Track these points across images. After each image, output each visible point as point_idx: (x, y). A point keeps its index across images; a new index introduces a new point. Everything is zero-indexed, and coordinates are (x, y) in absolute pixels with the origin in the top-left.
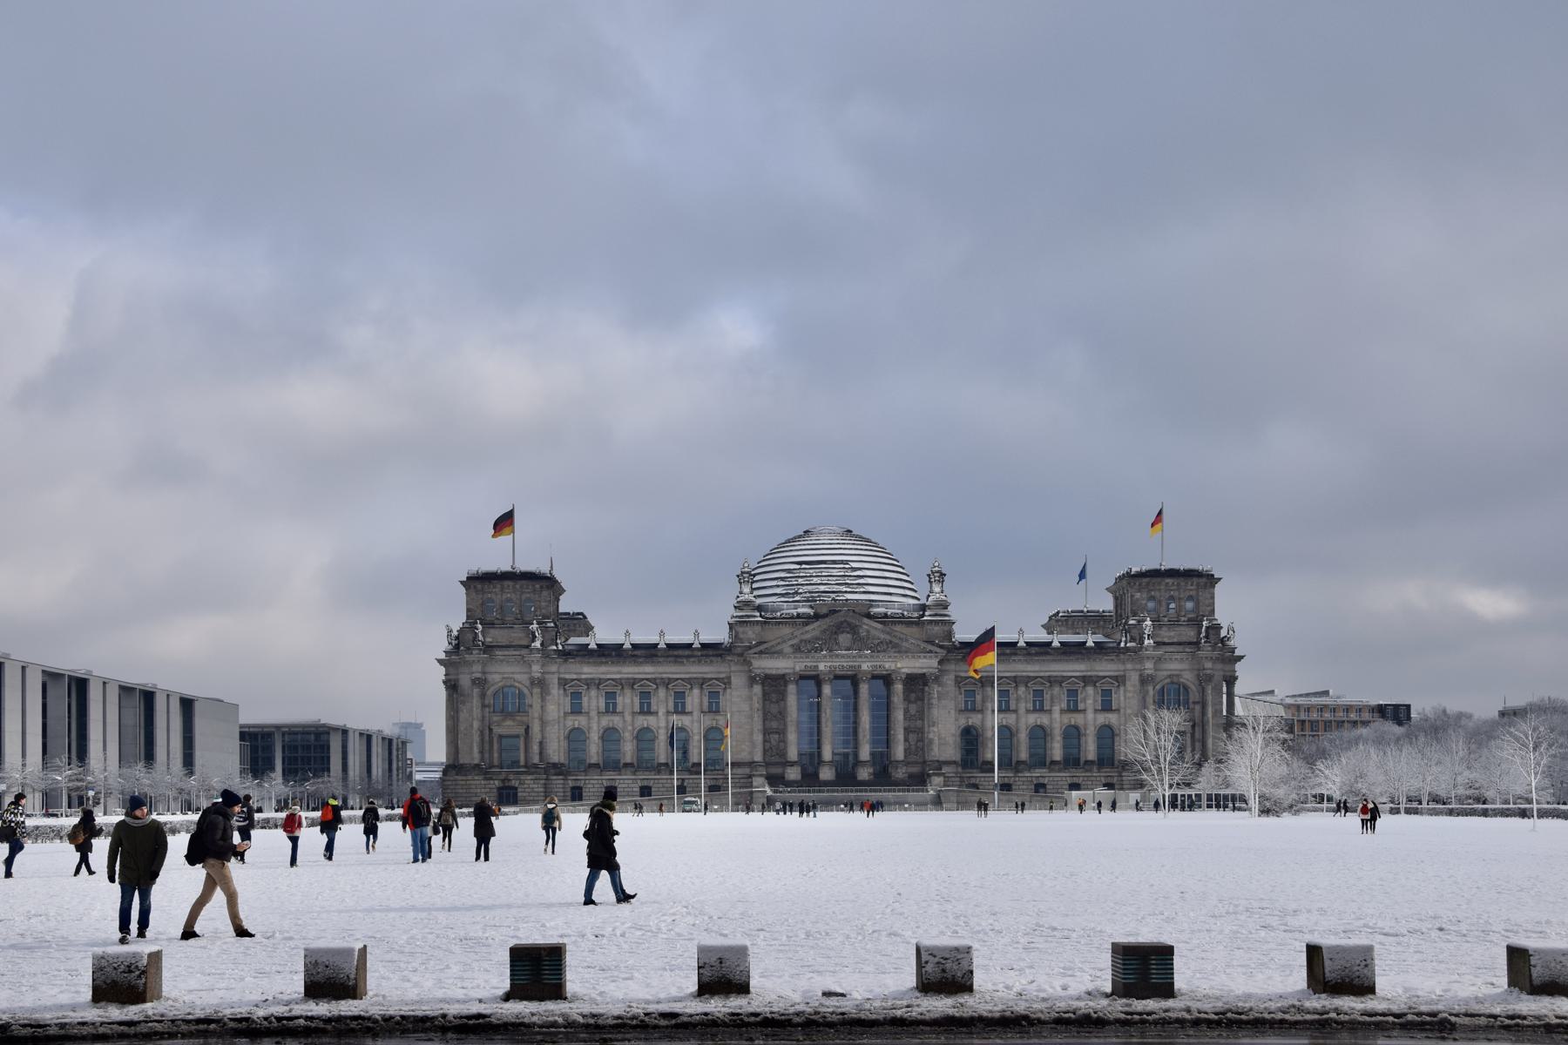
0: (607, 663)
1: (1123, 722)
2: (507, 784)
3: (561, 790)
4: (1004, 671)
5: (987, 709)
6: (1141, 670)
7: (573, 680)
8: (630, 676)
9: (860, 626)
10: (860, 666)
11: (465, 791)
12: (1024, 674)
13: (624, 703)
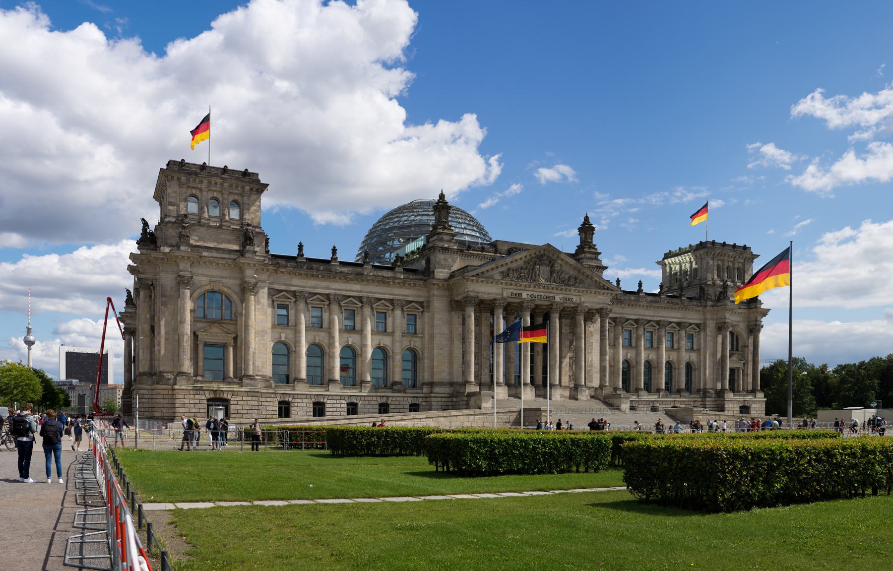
0: (318, 276)
1: (702, 359)
2: (218, 396)
3: (272, 404)
4: (631, 315)
5: (619, 344)
6: (717, 320)
7: (282, 291)
8: (338, 292)
9: (556, 260)
10: (554, 298)
11: (166, 401)
12: (644, 317)
13: (330, 319)
